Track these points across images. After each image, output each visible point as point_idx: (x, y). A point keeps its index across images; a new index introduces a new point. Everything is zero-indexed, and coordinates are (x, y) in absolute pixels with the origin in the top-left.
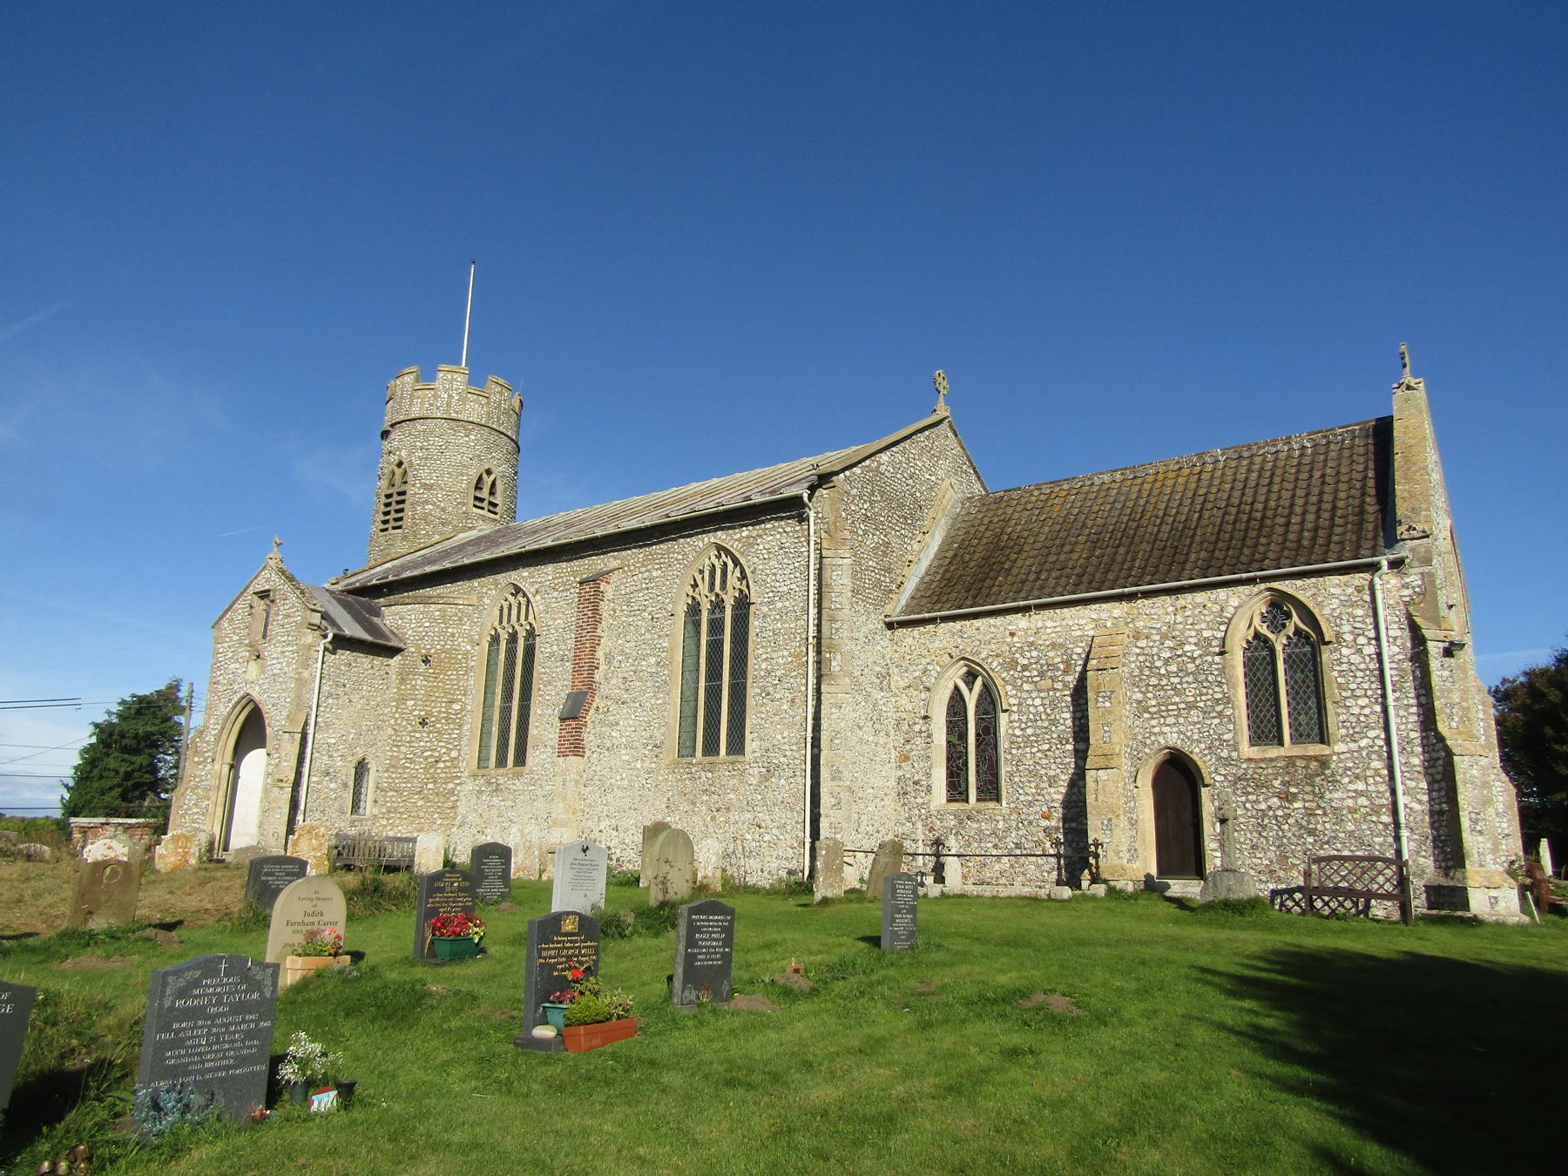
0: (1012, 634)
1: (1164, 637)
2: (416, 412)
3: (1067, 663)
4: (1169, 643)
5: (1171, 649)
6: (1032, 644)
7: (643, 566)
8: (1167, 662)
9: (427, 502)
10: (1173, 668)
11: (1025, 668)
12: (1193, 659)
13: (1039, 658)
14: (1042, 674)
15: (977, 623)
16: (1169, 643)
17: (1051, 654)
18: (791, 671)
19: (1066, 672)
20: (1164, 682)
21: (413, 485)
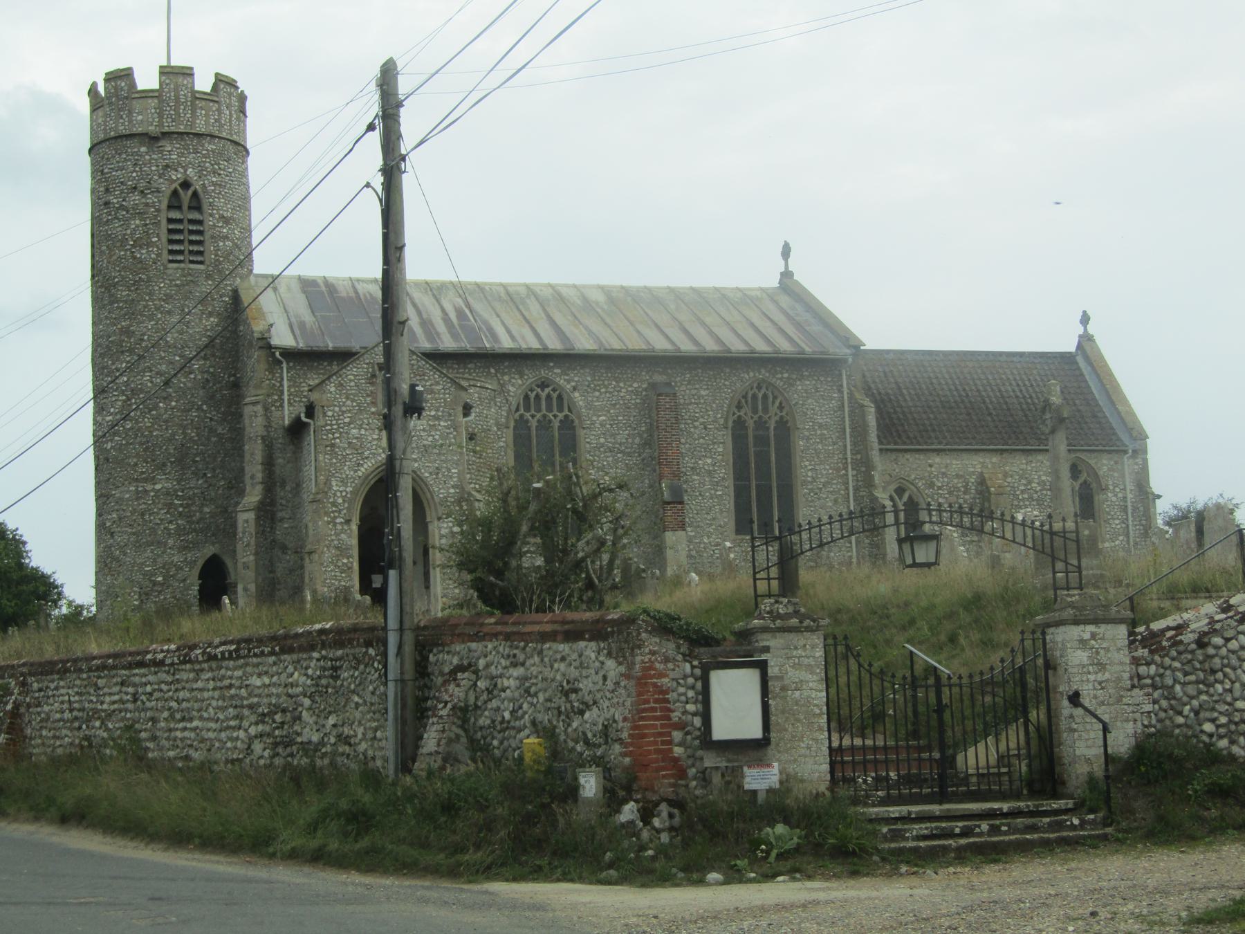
0: (931, 466)
1: (1021, 477)
2: (200, 126)
3: (966, 487)
4: (1024, 481)
5: (1025, 485)
6: (943, 474)
7: (689, 383)
8: (1023, 492)
9: (226, 238)
10: (1026, 496)
11: (939, 488)
12: (1037, 492)
13: (948, 483)
14: (950, 493)
15: (908, 456)
16: (1024, 481)
17: (956, 481)
18: (832, 479)
19: (965, 493)
20: (1021, 503)
21: (211, 215)
